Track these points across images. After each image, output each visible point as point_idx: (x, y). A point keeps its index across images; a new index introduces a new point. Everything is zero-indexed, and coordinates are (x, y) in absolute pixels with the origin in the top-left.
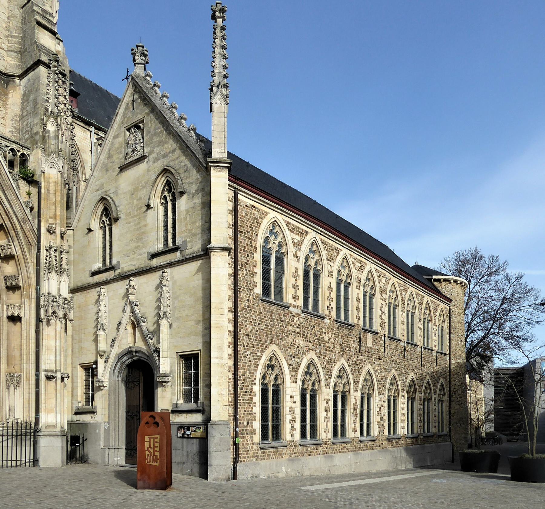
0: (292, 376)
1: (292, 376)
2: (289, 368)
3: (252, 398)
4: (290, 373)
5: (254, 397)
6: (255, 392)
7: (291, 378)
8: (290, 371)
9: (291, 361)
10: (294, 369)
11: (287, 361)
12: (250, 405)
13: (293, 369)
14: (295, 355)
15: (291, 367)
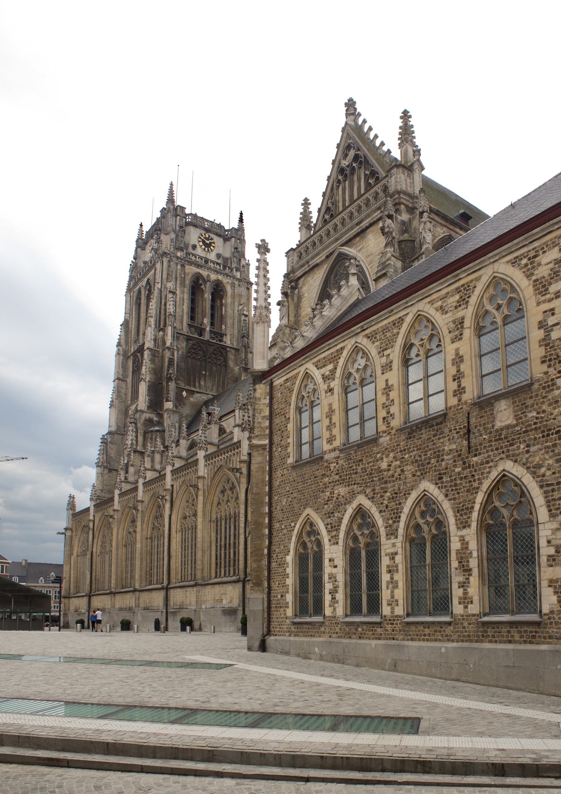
0: (332, 537)
1: (332, 537)
2: (326, 528)
3: (285, 569)
4: (329, 535)
5: (287, 569)
6: (288, 563)
7: (330, 540)
8: (329, 531)
9: (329, 520)
10: (333, 528)
11: (323, 521)
12: (283, 578)
13: (332, 527)
14: (334, 510)
15: (329, 526)
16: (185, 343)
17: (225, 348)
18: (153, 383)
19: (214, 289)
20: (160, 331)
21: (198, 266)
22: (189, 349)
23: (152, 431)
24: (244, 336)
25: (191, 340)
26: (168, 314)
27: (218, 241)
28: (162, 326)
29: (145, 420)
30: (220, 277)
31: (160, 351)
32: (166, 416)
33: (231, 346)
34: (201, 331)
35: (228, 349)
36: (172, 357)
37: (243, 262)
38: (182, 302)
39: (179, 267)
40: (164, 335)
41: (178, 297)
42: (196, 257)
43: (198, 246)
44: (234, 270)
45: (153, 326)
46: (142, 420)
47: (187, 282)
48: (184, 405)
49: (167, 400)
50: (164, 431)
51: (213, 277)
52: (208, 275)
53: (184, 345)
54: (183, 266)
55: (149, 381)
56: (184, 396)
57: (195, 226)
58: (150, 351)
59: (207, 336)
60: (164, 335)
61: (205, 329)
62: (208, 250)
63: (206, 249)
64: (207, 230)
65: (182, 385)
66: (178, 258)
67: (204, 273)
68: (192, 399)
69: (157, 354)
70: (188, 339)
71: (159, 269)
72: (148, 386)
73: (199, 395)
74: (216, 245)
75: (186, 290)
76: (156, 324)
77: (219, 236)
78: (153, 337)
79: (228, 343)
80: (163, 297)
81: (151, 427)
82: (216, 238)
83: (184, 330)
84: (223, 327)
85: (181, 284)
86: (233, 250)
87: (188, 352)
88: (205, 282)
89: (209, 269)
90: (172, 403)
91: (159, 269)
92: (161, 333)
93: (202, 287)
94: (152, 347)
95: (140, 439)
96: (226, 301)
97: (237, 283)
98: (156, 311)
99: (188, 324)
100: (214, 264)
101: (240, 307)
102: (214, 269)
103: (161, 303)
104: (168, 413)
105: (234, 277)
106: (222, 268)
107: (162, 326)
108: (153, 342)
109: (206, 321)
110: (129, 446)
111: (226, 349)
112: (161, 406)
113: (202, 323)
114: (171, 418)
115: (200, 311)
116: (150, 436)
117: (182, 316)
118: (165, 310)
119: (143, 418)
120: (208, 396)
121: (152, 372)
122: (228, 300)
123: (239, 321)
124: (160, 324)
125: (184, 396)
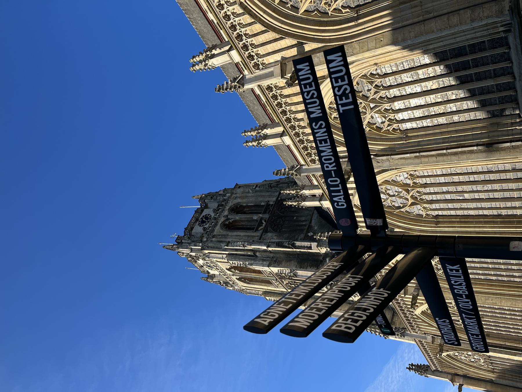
16: (268, 234)
19: (234, 213)
20: (256, 256)
22: (274, 230)
24: (270, 186)
25: (267, 229)
27: (206, 212)
30: (227, 208)
33: (277, 196)
35: (279, 199)
36: (275, 244)
37: (222, 192)
38: (238, 237)
39: (214, 239)
41: (234, 240)
42: (210, 227)
43: (205, 226)
44: (224, 198)
47: (224, 232)
51: (226, 213)
52: (224, 217)
53: (270, 234)
54: (214, 237)
57: (192, 229)
59: (267, 216)
62: (210, 219)
64: (197, 220)
65: (302, 236)
66: (207, 241)
67: (222, 219)
68: (316, 228)
69: (275, 259)
70: (266, 231)
73: (313, 221)
74: (208, 213)
75: (230, 234)
77: (202, 211)
79: (275, 199)
82: (204, 214)
84: (263, 204)
85: (225, 238)
86: (213, 200)
87: (276, 231)
88: (228, 219)
92: (258, 254)
93: (231, 221)
96: (245, 203)
97: (234, 195)
99: (255, 231)
100: (217, 213)
101: (251, 191)
103: (236, 254)
105: (229, 197)
109: (255, 217)
111: (279, 201)
113: (257, 221)
115: (249, 224)
117: (248, 236)
121: (288, 263)
122: (243, 202)
123: (260, 191)
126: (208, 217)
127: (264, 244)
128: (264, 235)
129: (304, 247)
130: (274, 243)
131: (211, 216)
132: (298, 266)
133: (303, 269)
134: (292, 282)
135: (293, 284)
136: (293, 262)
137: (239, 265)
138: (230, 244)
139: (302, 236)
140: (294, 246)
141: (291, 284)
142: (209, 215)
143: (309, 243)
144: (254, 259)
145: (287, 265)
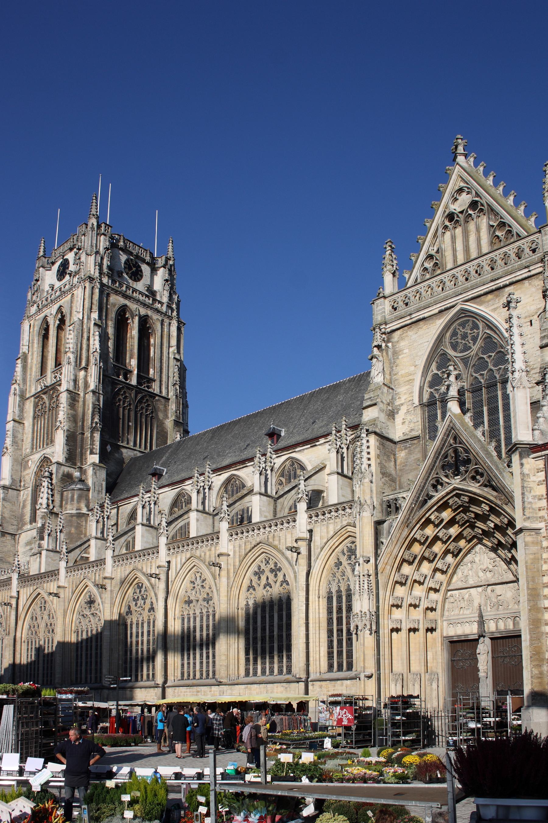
16: (110, 387)
17: (153, 396)
18: (72, 432)
21: (126, 296)
23: (73, 490)
26: (91, 351)
28: (83, 364)
29: (64, 475)
30: (150, 313)
31: (82, 394)
32: (90, 472)
34: (127, 373)
40: (86, 376)
45: (73, 364)
46: (60, 475)
47: (112, 315)
48: (109, 460)
49: (92, 453)
50: (88, 490)
55: (68, 430)
56: (109, 450)
58: (69, 394)
60: (86, 376)
61: (131, 372)
63: (133, 277)
67: (133, 306)
71: (80, 296)
72: (67, 436)
76: (76, 362)
78: (72, 377)
80: (85, 330)
81: (70, 485)
83: (110, 372)
89: (138, 301)
90: (98, 456)
91: (80, 296)
94: (71, 389)
95: (57, 498)
98: (77, 346)
102: (143, 301)
104: (94, 469)
106: (151, 302)
107: (83, 364)
108: (72, 383)
110: (45, 506)
111: (155, 398)
112: (83, 459)
114: (98, 474)
116: (70, 495)
118: (88, 346)
119: (61, 472)
120: (135, 452)
121: (72, 419)
124: (80, 362)
125: (109, 450)
126: (139, 276)
127: (96, 386)
128: (109, 381)
129: (92, 444)
130: (99, 400)
131: (139, 280)
132: (69, 433)
133: (66, 440)
134: (46, 407)
135: (42, 408)
136: (74, 425)
137: (68, 341)
138: (96, 329)
139: (107, 437)
140: (93, 430)
141: (42, 405)
142: (142, 276)
143: (98, 452)
144: (77, 366)
145: (69, 418)
